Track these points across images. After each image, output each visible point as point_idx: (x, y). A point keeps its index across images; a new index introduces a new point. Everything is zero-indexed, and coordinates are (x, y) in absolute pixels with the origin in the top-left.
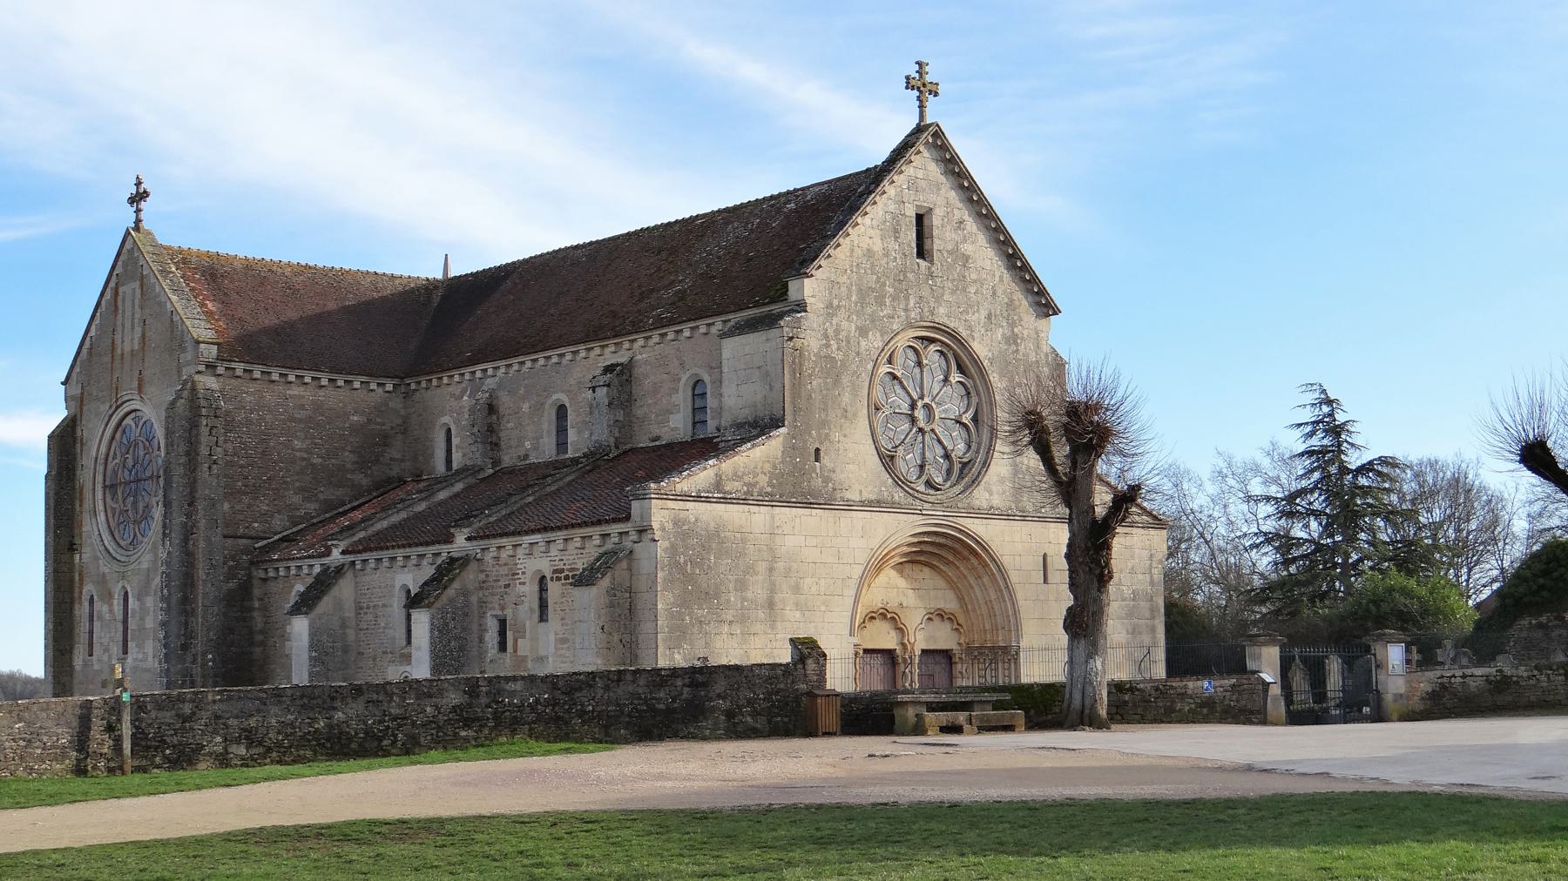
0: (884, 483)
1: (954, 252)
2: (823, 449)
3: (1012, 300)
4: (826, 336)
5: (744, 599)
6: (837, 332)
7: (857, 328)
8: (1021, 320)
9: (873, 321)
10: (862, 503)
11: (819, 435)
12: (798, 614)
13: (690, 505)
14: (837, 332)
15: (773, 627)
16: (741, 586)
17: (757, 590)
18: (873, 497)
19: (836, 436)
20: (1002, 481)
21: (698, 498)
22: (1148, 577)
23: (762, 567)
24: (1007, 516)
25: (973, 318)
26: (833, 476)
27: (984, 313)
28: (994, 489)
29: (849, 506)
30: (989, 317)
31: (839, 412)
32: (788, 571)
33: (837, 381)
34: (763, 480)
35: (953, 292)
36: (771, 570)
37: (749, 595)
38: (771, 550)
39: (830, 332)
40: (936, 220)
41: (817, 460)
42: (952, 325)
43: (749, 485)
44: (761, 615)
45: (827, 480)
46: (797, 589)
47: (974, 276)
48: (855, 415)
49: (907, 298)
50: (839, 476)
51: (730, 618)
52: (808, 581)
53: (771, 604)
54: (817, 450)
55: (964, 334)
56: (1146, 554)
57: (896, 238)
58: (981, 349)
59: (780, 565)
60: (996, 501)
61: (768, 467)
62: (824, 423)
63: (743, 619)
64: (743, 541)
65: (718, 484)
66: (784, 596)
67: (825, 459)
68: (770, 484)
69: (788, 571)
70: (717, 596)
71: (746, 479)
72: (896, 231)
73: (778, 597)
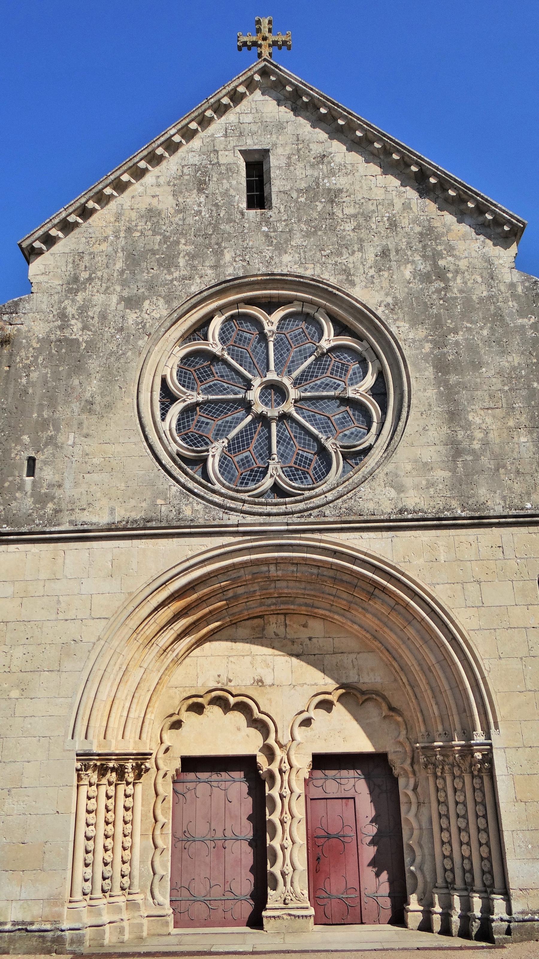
1: (313, 191)
2: (40, 458)
3: (431, 229)
6: (83, 310)
7: (122, 299)
14: (83, 310)
20: (427, 467)
24: (439, 523)
25: (349, 259)
26: (58, 493)
28: (408, 482)
29: (83, 535)
30: (385, 253)
31: (76, 406)
33: (78, 367)
35: (307, 235)
39: (71, 310)
40: (276, 162)
41: (31, 472)
42: (308, 273)
48: (109, 406)
50: (69, 491)
54: (32, 461)
55: (333, 281)
58: (366, 294)
60: (415, 500)
67: (46, 473)
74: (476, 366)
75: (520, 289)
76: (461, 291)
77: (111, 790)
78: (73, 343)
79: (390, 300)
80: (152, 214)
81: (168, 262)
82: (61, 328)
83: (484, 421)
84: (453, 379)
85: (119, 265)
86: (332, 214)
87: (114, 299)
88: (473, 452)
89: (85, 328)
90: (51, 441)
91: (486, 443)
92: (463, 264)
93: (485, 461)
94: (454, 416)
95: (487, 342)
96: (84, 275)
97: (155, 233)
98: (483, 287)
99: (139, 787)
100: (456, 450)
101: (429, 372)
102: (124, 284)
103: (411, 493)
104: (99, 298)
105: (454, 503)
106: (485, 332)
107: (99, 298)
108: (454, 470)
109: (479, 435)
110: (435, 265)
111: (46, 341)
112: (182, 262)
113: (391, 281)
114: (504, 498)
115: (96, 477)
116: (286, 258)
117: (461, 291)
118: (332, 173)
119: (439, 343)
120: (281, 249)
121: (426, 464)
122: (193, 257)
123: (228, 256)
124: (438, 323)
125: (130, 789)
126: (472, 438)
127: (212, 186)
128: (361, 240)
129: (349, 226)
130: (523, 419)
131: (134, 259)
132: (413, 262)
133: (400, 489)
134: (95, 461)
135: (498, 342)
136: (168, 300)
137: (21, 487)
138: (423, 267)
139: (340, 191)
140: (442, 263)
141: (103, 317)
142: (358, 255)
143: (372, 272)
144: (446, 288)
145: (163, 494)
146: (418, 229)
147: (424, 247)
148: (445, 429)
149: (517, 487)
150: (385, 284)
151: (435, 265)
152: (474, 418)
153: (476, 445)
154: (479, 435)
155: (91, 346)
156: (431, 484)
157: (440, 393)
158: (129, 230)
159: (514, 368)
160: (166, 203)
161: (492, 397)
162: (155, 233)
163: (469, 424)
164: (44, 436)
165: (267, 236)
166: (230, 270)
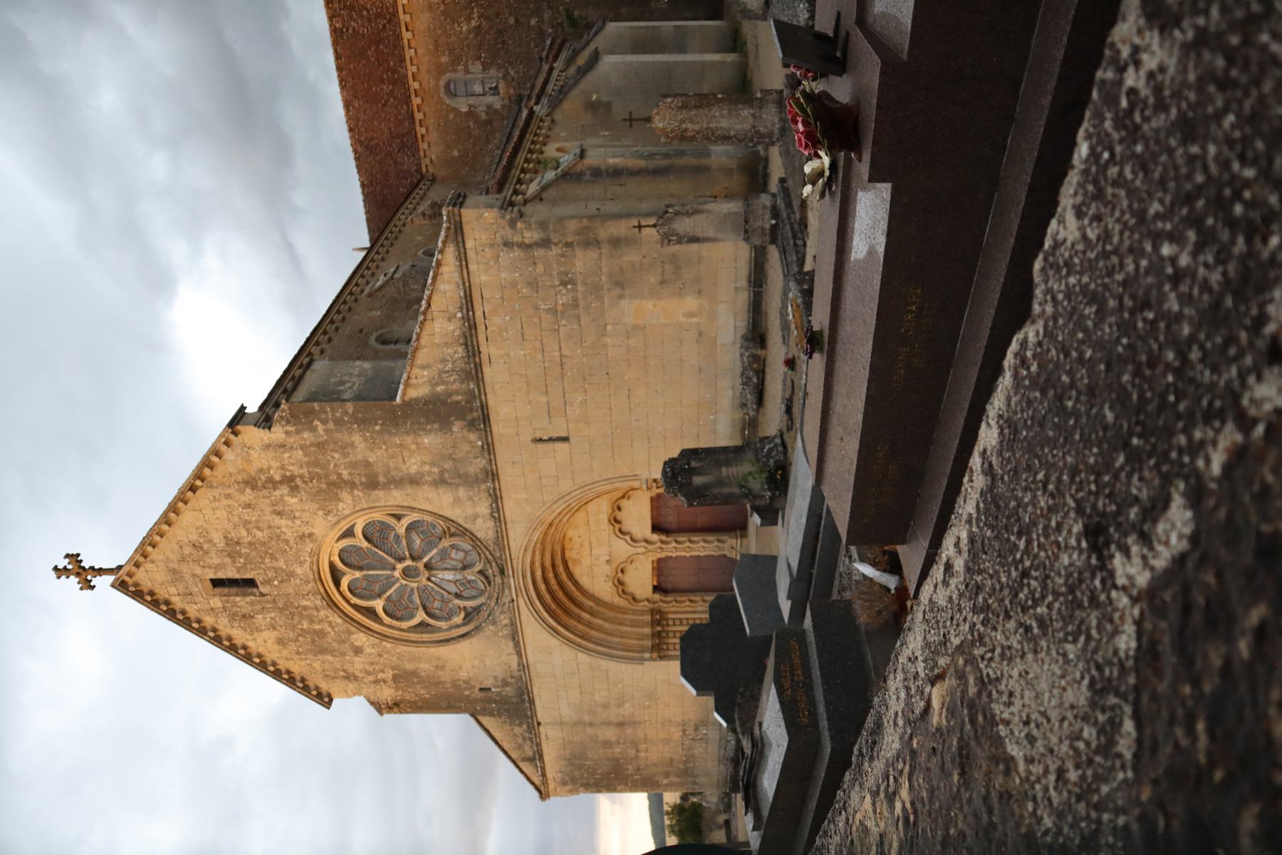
0: (495, 633)
3: (247, 483)
4: (376, 682)
5: (618, 743)
8: (261, 470)
9: (344, 642)
10: (519, 654)
11: (467, 689)
12: (627, 705)
13: (549, 776)
14: (369, 673)
15: (639, 723)
16: (607, 744)
17: (610, 734)
18: (511, 644)
19: (463, 675)
20: (457, 501)
21: (543, 769)
22: (539, 253)
23: (590, 731)
25: (289, 535)
26: (500, 677)
27: (278, 521)
28: (470, 512)
30: (279, 513)
31: (440, 673)
32: (591, 712)
33: (414, 673)
34: (517, 730)
36: (591, 725)
37: (614, 739)
38: (575, 724)
39: (371, 678)
43: (524, 738)
44: (629, 731)
45: (505, 683)
46: (606, 706)
47: (244, 533)
48: (438, 659)
49: (305, 608)
50: (500, 673)
51: (634, 752)
52: (597, 697)
53: (621, 725)
54: (481, 689)
56: (507, 257)
57: (252, 617)
59: (586, 718)
60: (484, 508)
61: (507, 727)
62: (455, 684)
63: (635, 744)
64: (571, 742)
65: (531, 760)
66: (613, 714)
67: (488, 683)
68: (520, 725)
69: (591, 712)
70: (618, 760)
71: (520, 741)
72: (244, 616)
73: (614, 719)
74: (368, 464)
75: (289, 428)
76: (301, 467)
77: (671, 635)
78: (395, 677)
79: (321, 513)
80: (281, 642)
81: (322, 634)
82: (385, 682)
83: (413, 465)
84: (382, 479)
85: (329, 657)
86: (250, 543)
87: (356, 659)
88: (442, 472)
89: (383, 671)
90: (467, 682)
91: (433, 464)
92: (274, 464)
93: (448, 465)
94: (414, 481)
95: (345, 455)
96: (342, 673)
97: (297, 640)
98: (294, 452)
99: (670, 616)
100: (440, 482)
101: (379, 493)
102: (343, 655)
103: (478, 510)
104: (358, 666)
105: (483, 487)
106: (337, 456)
107: (358, 666)
108: (458, 485)
109: (427, 468)
110: (281, 482)
111: (397, 689)
112: (317, 627)
113: (303, 511)
114: (476, 457)
115: (488, 663)
116: (299, 571)
117: (301, 467)
118: (210, 541)
119: (353, 485)
120: (292, 574)
121: (455, 500)
122: (311, 621)
123: (308, 603)
124: (331, 484)
125: (671, 622)
126: (430, 473)
127: (244, 611)
128: (270, 527)
129: (259, 534)
130: (409, 439)
131: (324, 651)
132: (282, 496)
133: (476, 516)
134: (477, 663)
135: (343, 448)
136: (350, 633)
137: (499, 693)
138: (284, 490)
139: (226, 537)
140: (277, 478)
141: (372, 664)
142: (284, 529)
143: (298, 522)
144: (302, 477)
145: (495, 633)
146: (248, 490)
147: (265, 488)
148: (426, 487)
149: (466, 448)
150: (308, 514)
151: (281, 482)
152: (413, 469)
153: (436, 470)
154: (427, 468)
155: (393, 669)
156: (470, 498)
157: (396, 488)
158: (298, 653)
159: (365, 440)
160: (271, 636)
161: (392, 457)
162: (297, 640)
163: (418, 473)
164: (463, 686)
165: (282, 581)
166: (318, 602)
